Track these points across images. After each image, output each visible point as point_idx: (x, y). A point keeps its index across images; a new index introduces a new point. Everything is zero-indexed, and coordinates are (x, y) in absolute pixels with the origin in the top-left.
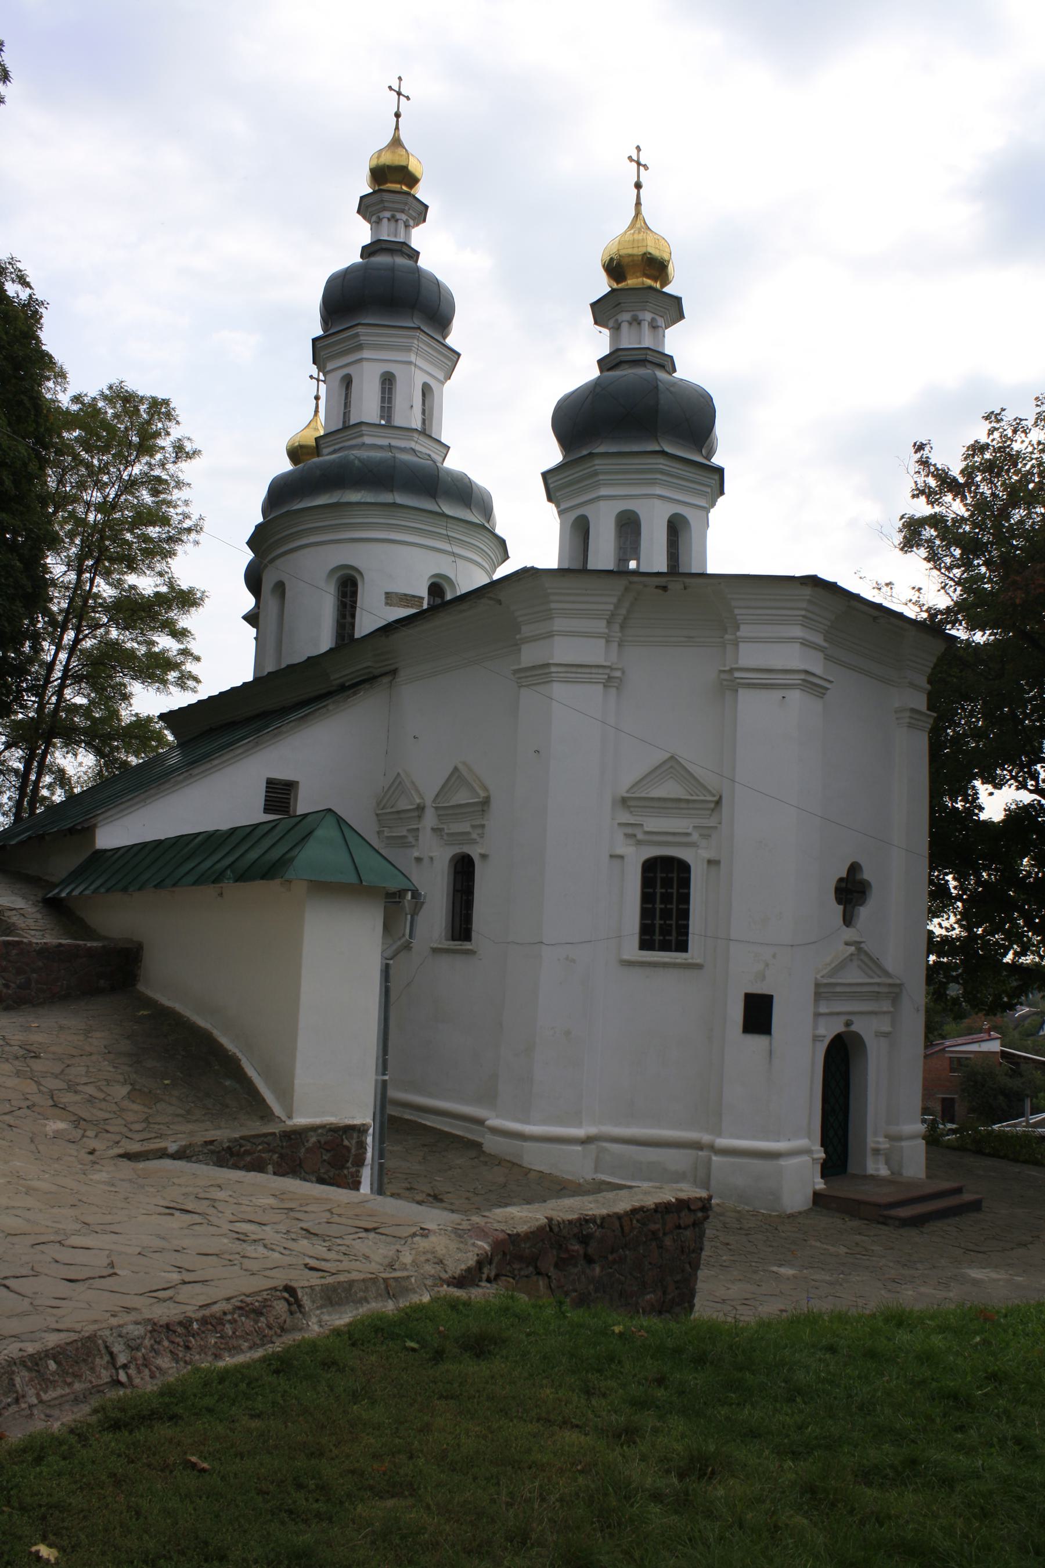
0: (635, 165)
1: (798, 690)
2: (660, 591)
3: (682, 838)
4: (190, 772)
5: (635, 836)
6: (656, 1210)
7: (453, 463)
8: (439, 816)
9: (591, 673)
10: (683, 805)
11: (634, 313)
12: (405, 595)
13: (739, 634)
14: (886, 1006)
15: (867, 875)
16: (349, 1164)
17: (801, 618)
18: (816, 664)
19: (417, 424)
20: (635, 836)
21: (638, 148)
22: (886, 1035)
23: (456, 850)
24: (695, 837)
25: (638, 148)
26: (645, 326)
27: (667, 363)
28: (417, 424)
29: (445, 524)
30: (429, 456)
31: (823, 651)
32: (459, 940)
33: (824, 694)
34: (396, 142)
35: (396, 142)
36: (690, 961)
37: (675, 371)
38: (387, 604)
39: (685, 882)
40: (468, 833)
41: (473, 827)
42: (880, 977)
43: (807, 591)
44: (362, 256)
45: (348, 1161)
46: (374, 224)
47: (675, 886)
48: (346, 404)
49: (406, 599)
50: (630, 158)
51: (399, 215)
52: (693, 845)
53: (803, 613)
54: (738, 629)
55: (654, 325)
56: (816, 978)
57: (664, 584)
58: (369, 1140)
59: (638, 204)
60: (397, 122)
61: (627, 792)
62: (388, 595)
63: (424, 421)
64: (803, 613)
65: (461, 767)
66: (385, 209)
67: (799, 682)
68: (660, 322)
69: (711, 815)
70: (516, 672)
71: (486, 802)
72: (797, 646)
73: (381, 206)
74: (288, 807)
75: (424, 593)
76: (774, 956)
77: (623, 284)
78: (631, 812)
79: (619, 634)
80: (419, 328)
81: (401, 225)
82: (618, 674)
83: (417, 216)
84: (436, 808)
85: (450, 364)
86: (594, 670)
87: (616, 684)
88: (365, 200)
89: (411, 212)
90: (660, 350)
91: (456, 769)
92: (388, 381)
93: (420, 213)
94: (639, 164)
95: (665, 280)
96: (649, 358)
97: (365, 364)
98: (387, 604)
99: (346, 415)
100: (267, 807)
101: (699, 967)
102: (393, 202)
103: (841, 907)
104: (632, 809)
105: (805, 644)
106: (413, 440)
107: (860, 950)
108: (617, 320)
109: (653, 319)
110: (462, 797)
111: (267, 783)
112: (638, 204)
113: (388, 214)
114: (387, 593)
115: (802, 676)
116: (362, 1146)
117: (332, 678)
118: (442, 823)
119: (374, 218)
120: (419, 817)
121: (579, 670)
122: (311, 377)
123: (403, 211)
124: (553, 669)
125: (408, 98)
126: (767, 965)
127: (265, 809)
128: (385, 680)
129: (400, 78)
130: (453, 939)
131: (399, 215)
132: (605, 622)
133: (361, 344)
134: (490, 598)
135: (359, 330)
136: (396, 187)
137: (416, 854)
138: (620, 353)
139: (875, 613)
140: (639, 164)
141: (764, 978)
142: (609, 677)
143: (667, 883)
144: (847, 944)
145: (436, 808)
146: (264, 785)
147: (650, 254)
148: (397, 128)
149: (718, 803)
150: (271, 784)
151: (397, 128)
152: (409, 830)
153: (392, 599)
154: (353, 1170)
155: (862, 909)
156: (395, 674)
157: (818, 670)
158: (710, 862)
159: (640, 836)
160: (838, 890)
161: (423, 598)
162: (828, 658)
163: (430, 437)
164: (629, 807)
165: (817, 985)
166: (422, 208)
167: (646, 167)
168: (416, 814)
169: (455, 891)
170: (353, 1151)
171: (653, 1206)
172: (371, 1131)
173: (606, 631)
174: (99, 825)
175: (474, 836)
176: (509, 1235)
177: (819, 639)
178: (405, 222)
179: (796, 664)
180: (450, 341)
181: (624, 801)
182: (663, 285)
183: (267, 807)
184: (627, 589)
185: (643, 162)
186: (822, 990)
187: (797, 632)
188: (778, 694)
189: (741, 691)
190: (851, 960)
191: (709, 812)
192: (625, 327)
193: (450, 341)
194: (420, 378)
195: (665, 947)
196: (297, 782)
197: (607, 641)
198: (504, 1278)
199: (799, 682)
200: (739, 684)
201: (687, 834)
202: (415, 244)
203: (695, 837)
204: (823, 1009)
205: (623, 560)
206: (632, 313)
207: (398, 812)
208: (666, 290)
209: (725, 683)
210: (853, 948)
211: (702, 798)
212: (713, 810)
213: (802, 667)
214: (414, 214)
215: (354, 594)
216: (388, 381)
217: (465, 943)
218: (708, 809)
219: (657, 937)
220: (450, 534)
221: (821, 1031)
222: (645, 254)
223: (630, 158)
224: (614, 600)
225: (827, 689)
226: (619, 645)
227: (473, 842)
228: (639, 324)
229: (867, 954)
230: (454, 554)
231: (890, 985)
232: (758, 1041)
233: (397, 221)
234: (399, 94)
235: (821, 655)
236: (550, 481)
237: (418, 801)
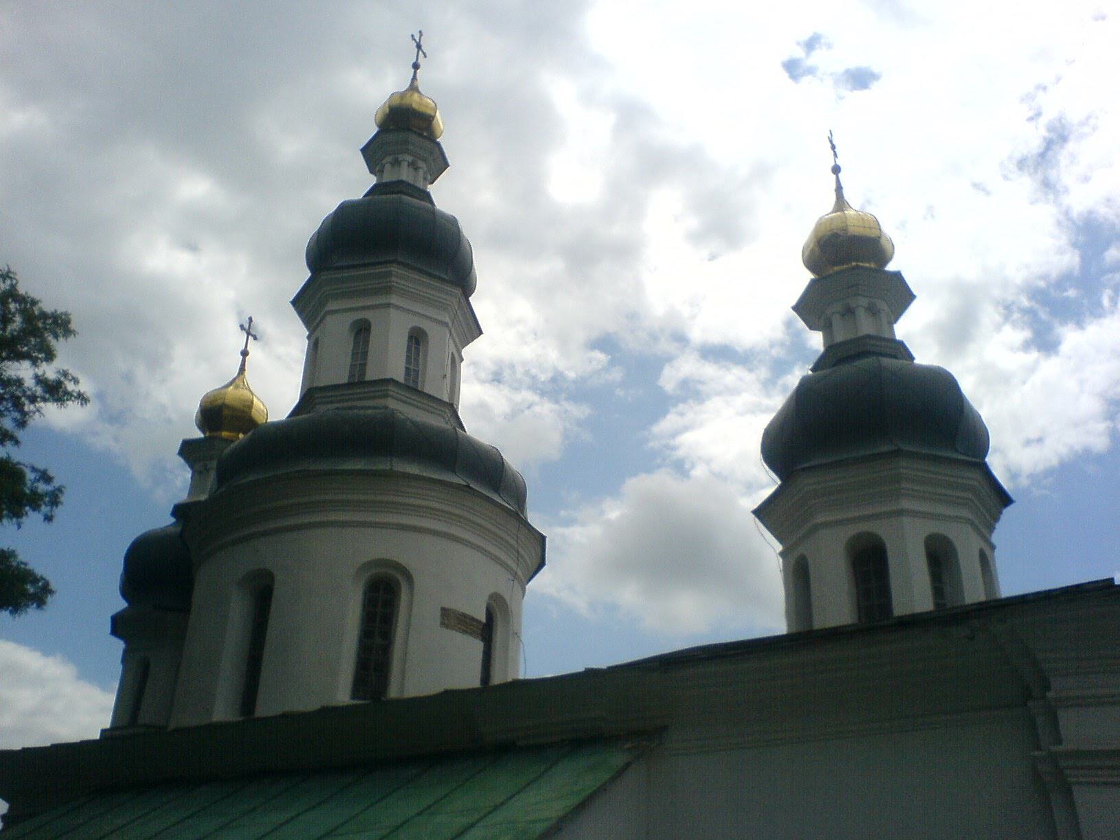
12: (464, 615)
34: (413, 88)
35: (413, 88)
62: (445, 612)
97: (392, 311)
98: (443, 624)
106: (444, 418)
114: (443, 609)
123: (425, 160)
133: (390, 287)
135: (394, 269)
148: (414, 78)
151: (414, 78)
216: (417, 339)
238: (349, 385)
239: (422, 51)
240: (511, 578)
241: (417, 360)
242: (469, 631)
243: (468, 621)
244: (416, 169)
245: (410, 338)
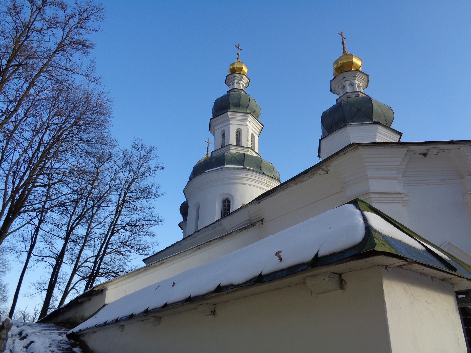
2: (422, 156)
9: (394, 197)
19: (250, 146)
28: (250, 146)
29: (265, 179)
48: (223, 138)
51: (240, 82)
57: (424, 152)
80: (250, 113)
85: (260, 129)
86: (395, 196)
88: (228, 77)
121: (386, 196)
124: (372, 196)
131: (240, 82)
134: (323, 170)
138: (348, 94)
178: (242, 84)
184: (406, 155)
206: (350, 81)
220: (267, 183)
244: (239, 84)
245: (237, 132)
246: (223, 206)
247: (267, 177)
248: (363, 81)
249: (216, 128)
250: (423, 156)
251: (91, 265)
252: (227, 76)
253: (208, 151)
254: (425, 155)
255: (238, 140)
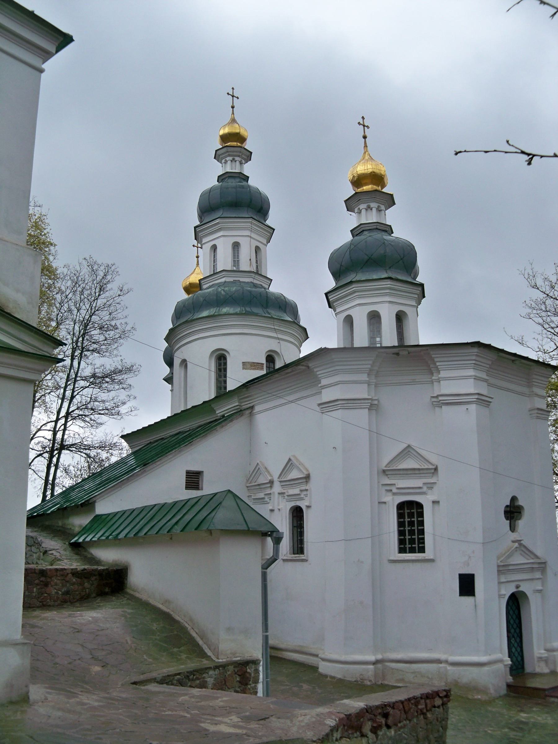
0: (362, 127)
1: (475, 404)
2: (396, 356)
3: (418, 490)
4: (144, 470)
5: (391, 490)
6: (421, 698)
7: (274, 289)
8: (282, 485)
10: (417, 472)
11: (368, 204)
12: (254, 363)
13: (440, 376)
14: (538, 575)
15: (521, 502)
16: (251, 682)
17: (473, 365)
18: (484, 389)
20: (391, 490)
21: (363, 118)
22: (540, 591)
23: (293, 504)
24: (425, 489)
25: (363, 118)
26: (374, 210)
27: (389, 230)
29: (273, 323)
30: (261, 285)
31: (486, 382)
32: (298, 554)
33: (489, 405)
34: (233, 121)
35: (233, 121)
36: (427, 558)
37: (393, 233)
38: (244, 368)
39: (421, 514)
40: (299, 495)
41: (301, 491)
42: (533, 559)
43: (475, 350)
44: (218, 181)
45: (250, 681)
46: (223, 164)
47: (415, 517)
49: (255, 366)
50: (359, 123)
52: (424, 493)
53: (474, 362)
54: (439, 372)
55: (380, 209)
56: (497, 563)
57: (397, 352)
58: (261, 669)
59: (366, 146)
60: (233, 110)
61: (386, 467)
63: (257, 266)
64: (474, 362)
65: (292, 458)
66: (229, 156)
67: (475, 400)
68: (383, 207)
69: (432, 477)
70: (319, 405)
71: (307, 478)
72: (473, 379)
73: (227, 154)
74: (198, 486)
75: (264, 361)
76: (473, 552)
77: (361, 189)
78: (388, 478)
79: (375, 381)
81: (238, 163)
82: (376, 402)
83: (246, 158)
84: (280, 482)
86: (363, 401)
87: (375, 408)
89: (243, 156)
90: (384, 222)
91: (290, 460)
92: (236, 246)
93: (248, 156)
94: (364, 126)
95: (383, 186)
96: (378, 227)
98: (244, 368)
99: (215, 266)
100: (187, 486)
101: (432, 561)
102: (233, 152)
103: (508, 521)
104: (389, 476)
105: (476, 378)
106: (252, 278)
107: (520, 545)
108: (359, 208)
109: (379, 206)
110: (294, 474)
111: (186, 473)
112: (366, 146)
113: (231, 158)
114: (243, 363)
115: (476, 397)
116: (257, 671)
117: (217, 412)
118: (284, 490)
119: (223, 161)
120: (271, 487)
122: (194, 246)
123: (239, 156)
125: (238, 98)
126: (470, 557)
127: (186, 487)
128: (248, 412)
129: (233, 88)
130: (294, 554)
132: (366, 374)
134: (303, 365)
136: (235, 144)
137: (271, 508)
138: (362, 226)
139: (513, 358)
140: (364, 126)
141: (468, 565)
142: (371, 405)
143: (411, 515)
144: (513, 542)
145: (280, 482)
146: (185, 474)
147: (374, 172)
148: (233, 113)
149: (436, 469)
150: (189, 474)
151: (233, 113)
152: (265, 495)
153: (246, 365)
154: (253, 685)
155: (519, 521)
156: (252, 408)
157: (484, 392)
158: (434, 502)
159: (395, 490)
160: (506, 512)
161: (263, 364)
162: (490, 385)
163: (261, 275)
164: (387, 475)
165: (498, 566)
166: (249, 153)
167: (368, 127)
168: (269, 485)
169: (293, 527)
170: (253, 675)
171: (420, 696)
172: (261, 663)
173: (367, 379)
174: (97, 501)
175: (302, 496)
176: (345, 715)
177: (484, 375)
178: (240, 162)
179: (472, 391)
180: (268, 222)
181: (384, 471)
182: (382, 189)
183: (187, 486)
185: (366, 125)
186: (501, 569)
187: (471, 372)
188: (464, 407)
189: (443, 407)
190: (516, 551)
191: (431, 475)
192: (363, 211)
193: (268, 222)
194: (255, 243)
195: (412, 551)
196: (203, 472)
197: (369, 385)
198: (344, 739)
199: (475, 400)
200: (442, 403)
201: (420, 488)
202: (246, 173)
203: (425, 489)
204: (503, 580)
205: (372, 338)
206: (367, 204)
207: (259, 485)
208: (384, 190)
209: (434, 403)
210: (517, 544)
211: (426, 467)
212: (433, 473)
213: (476, 392)
214: (245, 157)
215: (225, 364)
216: (236, 246)
217: (301, 555)
218: (430, 473)
219: (408, 546)
220: (276, 327)
221: (503, 592)
222: (371, 172)
223: (359, 123)
224: (371, 362)
225: (490, 402)
226: (375, 386)
227: (302, 499)
228: (371, 209)
229: (525, 547)
230: (278, 338)
231: (539, 563)
232: (468, 600)
233: (236, 161)
234: (233, 96)
235: (485, 384)
236: (330, 297)
237: (270, 478)
238: (215, 274)
239: (235, 97)
240: (278, 341)
241: (238, 256)
242: (256, 368)
243: (255, 364)
246: (217, 365)
247: (275, 321)
248: (385, 201)
249: (204, 240)
250: (396, 356)
251: (49, 435)
252: (216, 151)
253: (198, 262)
254: (398, 354)
255: (236, 260)
